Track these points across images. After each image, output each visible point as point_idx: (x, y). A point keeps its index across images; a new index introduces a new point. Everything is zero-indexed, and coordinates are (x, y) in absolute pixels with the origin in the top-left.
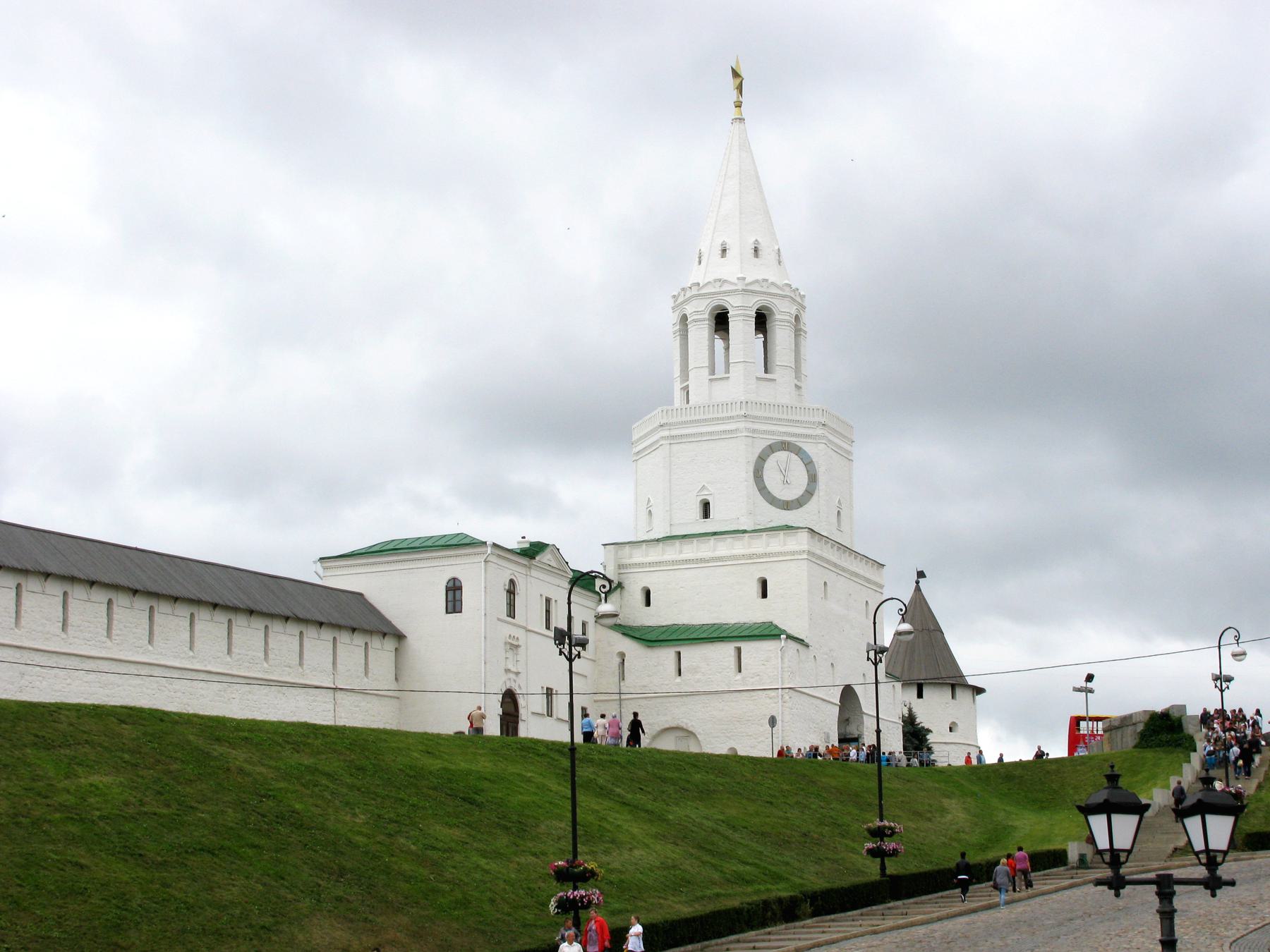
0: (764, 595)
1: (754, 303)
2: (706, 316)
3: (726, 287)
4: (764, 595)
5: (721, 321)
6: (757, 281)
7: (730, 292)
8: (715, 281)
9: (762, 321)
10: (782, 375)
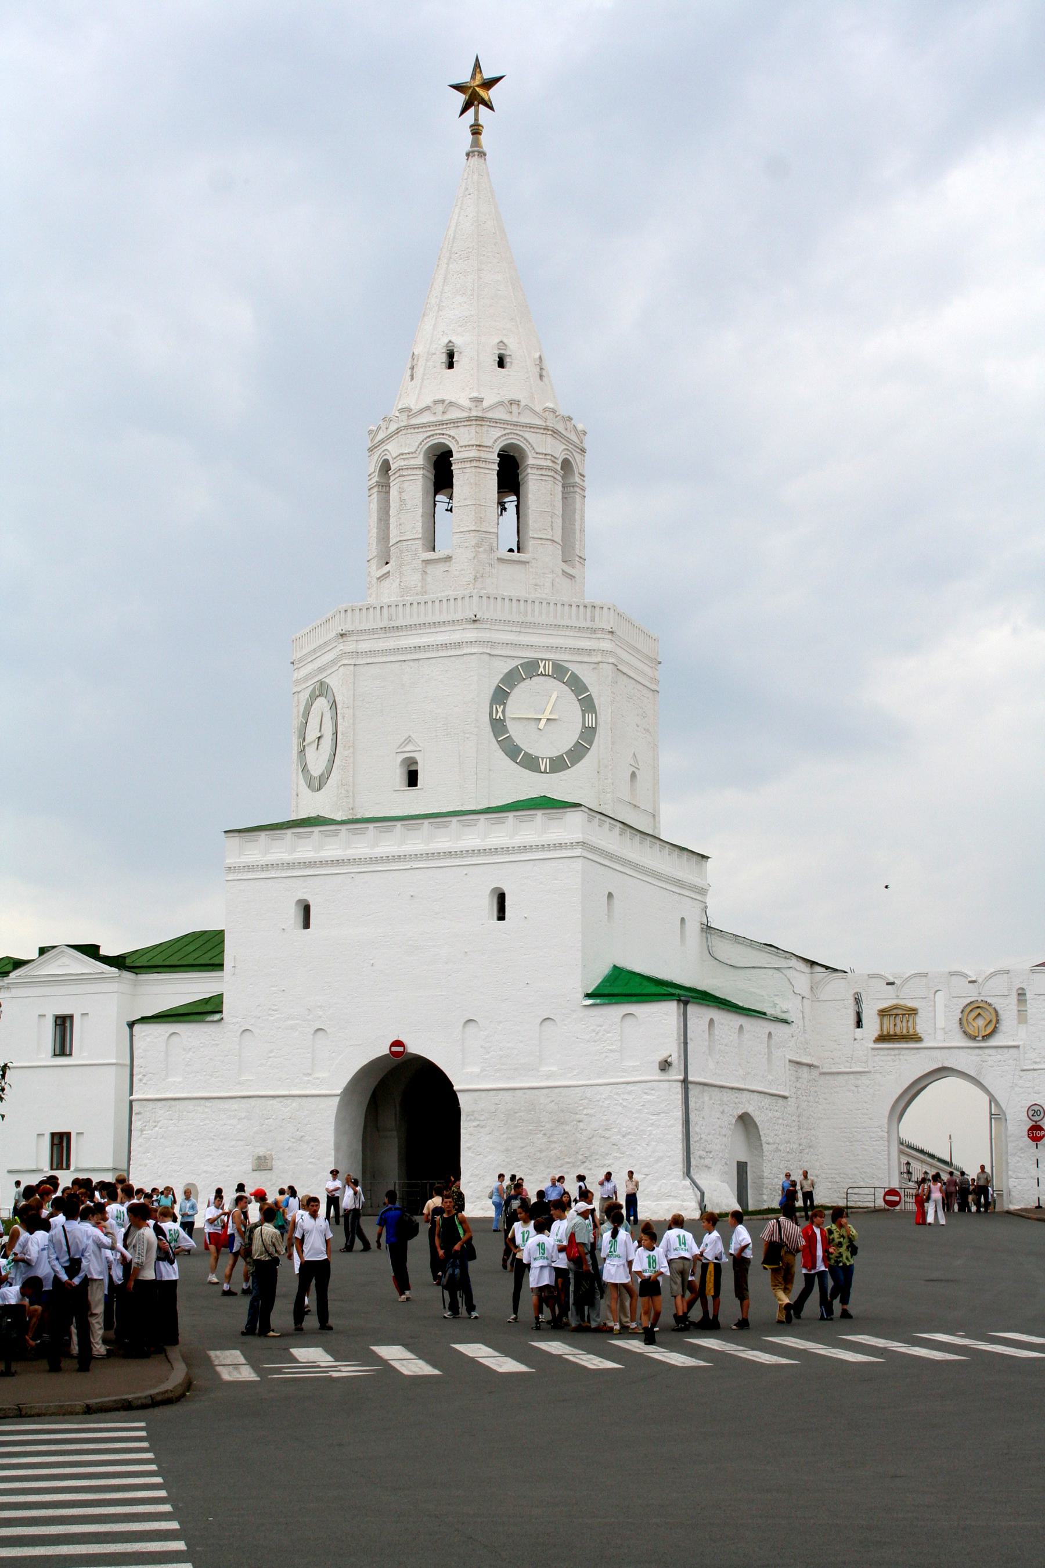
0: (501, 917)
1: (495, 440)
2: (420, 460)
3: (454, 414)
4: (501, 917)
5: (441, 471)
6: (501, 403)
7: (455, 423)
8: (436, 402)
9: (510, 473)
10: (543, 554)
